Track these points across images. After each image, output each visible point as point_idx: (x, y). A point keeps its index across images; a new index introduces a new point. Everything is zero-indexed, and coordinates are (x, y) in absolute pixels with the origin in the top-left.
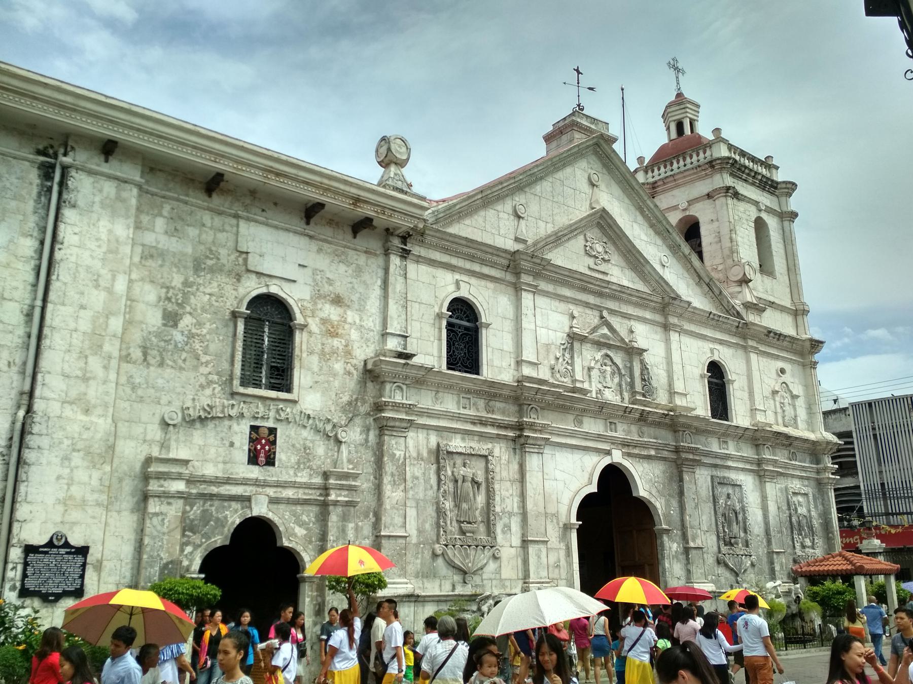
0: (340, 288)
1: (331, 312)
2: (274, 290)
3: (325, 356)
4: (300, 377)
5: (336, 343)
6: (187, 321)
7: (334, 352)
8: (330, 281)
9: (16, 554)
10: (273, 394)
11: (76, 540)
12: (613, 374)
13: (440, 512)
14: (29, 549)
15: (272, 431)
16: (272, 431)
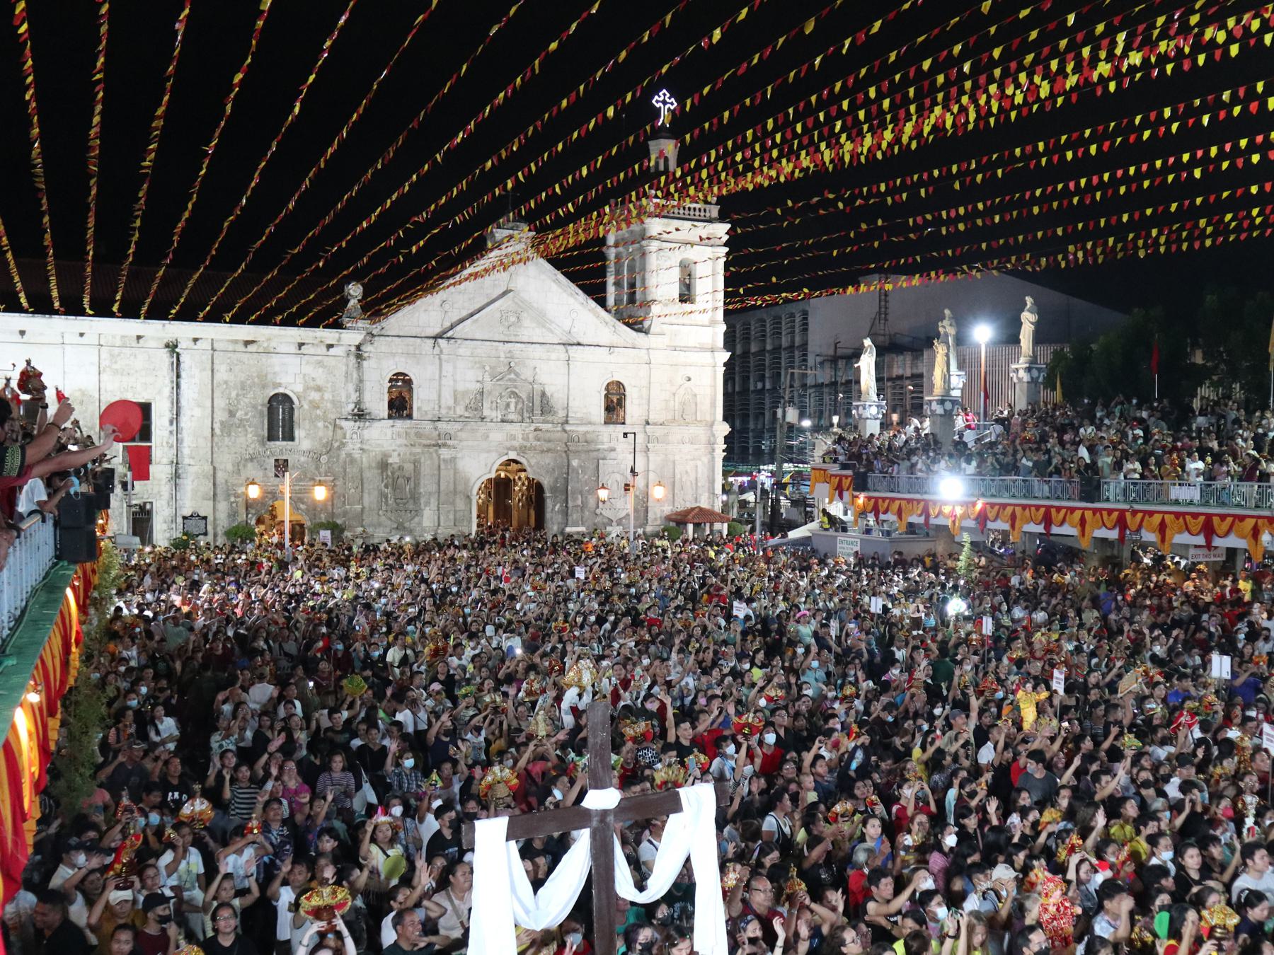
0: (320, 382)
1: (314, 396)
2: (281, 390)
3: (313, 421)
4: (298, 433)
5: (318, 412)
6: (239, 414)
7: (318, 417)
8: (314, 379)
9: (180, 520)
10: (285, 443)
11: (202, 514)
12: (516, 403)
13: (383, 496)
14: (185, 518)
15: (286, 461)
16: (286, 461)
